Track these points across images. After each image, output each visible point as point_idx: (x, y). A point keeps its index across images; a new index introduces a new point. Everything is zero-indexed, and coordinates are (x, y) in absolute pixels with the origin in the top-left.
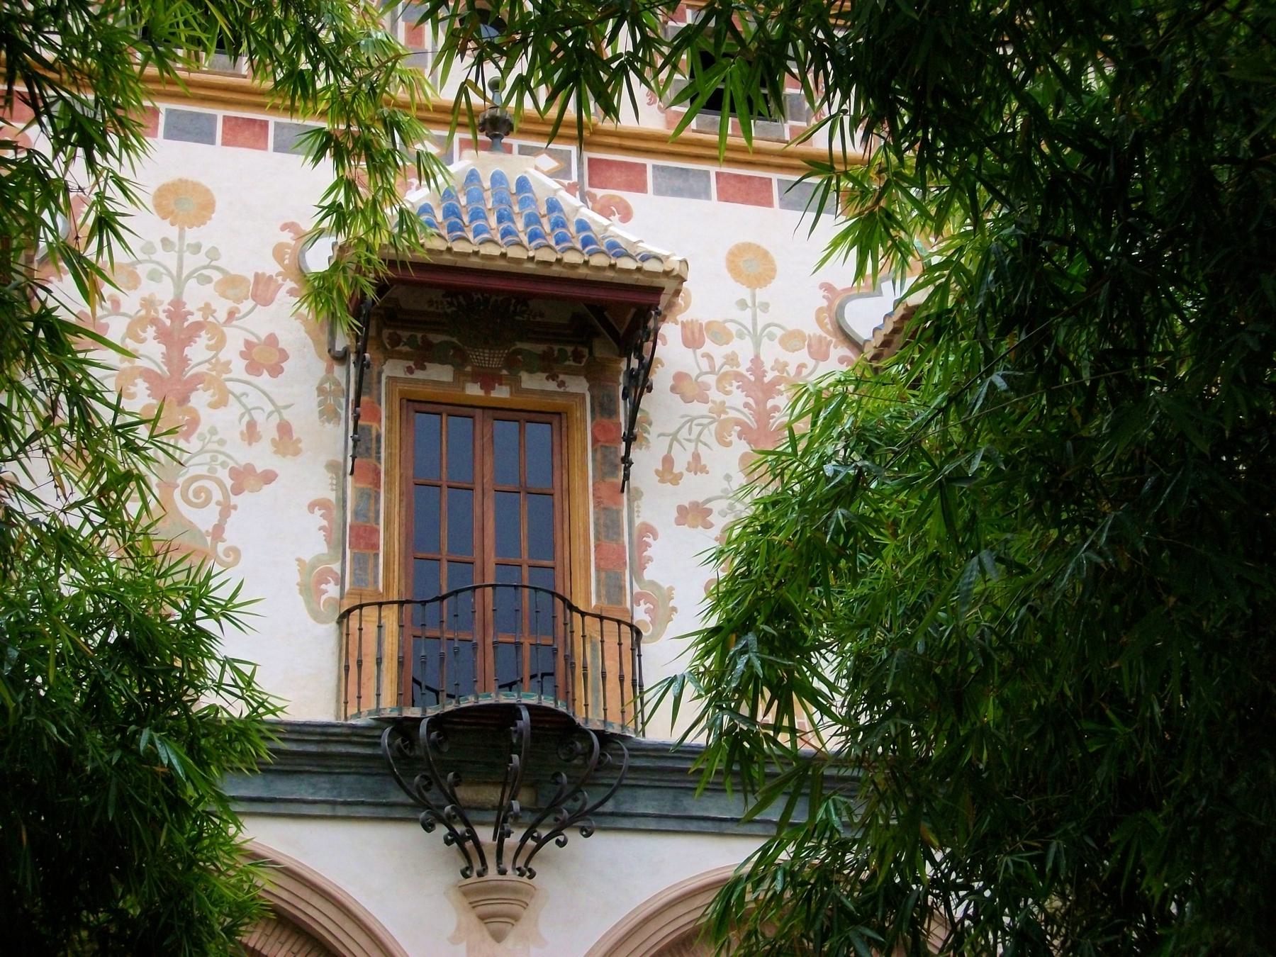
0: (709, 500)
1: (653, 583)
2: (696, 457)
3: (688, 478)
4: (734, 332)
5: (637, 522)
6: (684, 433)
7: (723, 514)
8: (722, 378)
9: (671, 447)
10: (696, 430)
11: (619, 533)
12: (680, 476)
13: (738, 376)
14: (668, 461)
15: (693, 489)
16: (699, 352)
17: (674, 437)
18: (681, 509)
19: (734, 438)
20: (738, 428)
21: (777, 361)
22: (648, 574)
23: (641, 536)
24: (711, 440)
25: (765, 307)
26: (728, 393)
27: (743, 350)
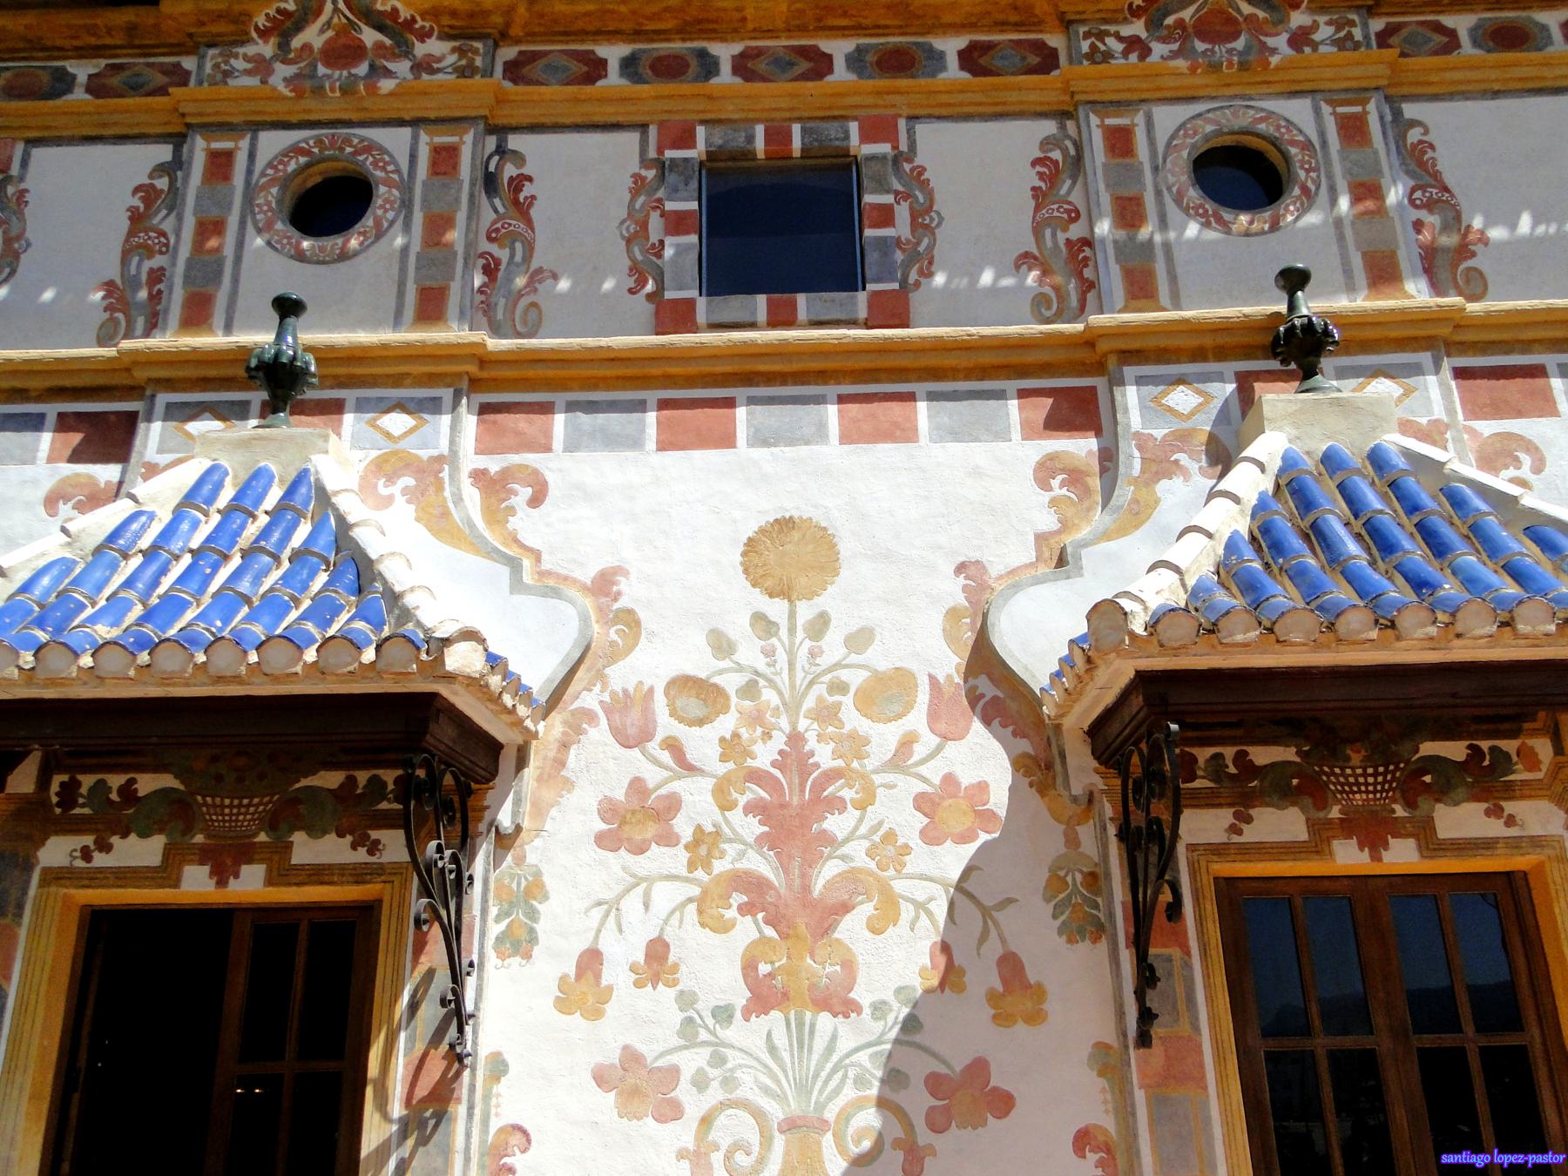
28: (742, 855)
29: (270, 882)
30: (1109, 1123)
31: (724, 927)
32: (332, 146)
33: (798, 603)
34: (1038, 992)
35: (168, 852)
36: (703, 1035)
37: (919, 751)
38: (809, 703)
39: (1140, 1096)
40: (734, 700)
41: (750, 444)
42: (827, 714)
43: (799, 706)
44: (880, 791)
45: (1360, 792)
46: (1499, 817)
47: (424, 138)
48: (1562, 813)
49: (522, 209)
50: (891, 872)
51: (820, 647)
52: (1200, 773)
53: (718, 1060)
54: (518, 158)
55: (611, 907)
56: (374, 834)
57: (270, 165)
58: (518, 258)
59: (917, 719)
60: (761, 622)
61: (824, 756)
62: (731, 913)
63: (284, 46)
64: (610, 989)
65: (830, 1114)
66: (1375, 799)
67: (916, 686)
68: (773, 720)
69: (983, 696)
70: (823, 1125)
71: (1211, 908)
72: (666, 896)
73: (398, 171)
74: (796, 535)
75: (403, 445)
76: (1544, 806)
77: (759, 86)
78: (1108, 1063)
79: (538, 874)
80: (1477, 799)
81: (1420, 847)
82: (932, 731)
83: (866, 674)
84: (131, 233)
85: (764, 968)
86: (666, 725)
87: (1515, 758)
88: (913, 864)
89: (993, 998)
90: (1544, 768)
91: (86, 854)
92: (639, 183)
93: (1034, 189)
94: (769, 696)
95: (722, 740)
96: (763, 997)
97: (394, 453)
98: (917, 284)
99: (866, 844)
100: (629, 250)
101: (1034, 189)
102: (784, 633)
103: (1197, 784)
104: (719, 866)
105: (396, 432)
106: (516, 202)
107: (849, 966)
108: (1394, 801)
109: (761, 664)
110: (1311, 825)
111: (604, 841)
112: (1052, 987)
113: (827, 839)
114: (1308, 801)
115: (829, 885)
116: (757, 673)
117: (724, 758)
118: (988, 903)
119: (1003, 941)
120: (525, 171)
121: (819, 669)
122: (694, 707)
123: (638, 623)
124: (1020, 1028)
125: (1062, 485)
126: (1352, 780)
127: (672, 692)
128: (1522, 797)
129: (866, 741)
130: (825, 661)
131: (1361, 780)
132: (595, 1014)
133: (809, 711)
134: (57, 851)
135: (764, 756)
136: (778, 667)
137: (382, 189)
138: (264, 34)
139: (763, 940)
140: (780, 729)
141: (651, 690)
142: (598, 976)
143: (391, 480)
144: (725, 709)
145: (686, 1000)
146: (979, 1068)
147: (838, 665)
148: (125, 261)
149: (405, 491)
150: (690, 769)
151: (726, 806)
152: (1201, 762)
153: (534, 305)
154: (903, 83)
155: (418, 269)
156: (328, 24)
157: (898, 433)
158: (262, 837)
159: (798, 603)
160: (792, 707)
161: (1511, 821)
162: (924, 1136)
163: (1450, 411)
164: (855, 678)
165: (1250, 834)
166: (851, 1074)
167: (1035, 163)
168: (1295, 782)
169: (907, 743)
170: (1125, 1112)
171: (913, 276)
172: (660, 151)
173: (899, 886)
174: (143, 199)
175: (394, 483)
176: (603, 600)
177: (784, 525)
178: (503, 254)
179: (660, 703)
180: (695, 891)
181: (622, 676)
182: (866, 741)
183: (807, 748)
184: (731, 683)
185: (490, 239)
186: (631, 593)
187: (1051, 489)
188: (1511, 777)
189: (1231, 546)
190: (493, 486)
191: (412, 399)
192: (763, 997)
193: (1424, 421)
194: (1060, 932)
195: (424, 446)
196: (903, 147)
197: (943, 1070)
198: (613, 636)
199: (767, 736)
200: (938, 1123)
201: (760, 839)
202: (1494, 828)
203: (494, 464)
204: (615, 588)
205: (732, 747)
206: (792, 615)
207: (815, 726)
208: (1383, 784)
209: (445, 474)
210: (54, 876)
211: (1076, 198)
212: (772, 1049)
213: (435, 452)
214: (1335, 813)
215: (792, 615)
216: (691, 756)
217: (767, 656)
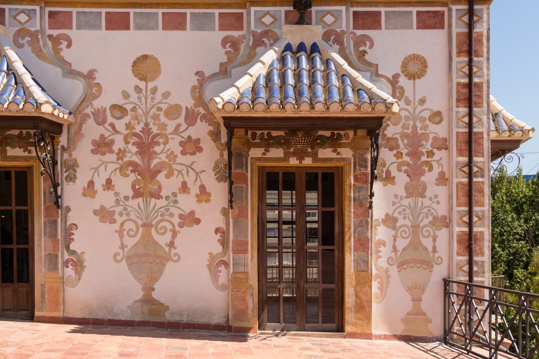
28: (131, 157)
30: (224, 227)
31: (127, 176)
33: (148, 83)
34: (209, 195)
36: (121, 203)
37: (182, 129)
38: (151, 114)
39: (231, 220)
40: (129, 112)
41: (135, 29)
42: (156, 117)
43: (148, 114)
44: (170, 140)
45: (300, 144)
46: (335, 152)
48: (352, 152)
50: (172, 162)
51: (155, 97)
52: (257, 138)
53: (125, 209)
55: (96, 169)
56: (29, 148)
59: (181, 120)
60: (138, 89)
61: (155, 130)
62: (129, 172)
64: (97, 191)
65: (154, 223)
66: (303, 146)
67: (182, 109)
68: (140, 119)
69: (201, 113)
70: (152, 226)
71: (256, 175)
72: (111, 167)
74: (148, 61)
75: (25, 26)
76: (348, 150)
78: (225, 212)
79: (76, 160)
80: (330, 147)
81: (313, 160)
82: (186, 123)
83: (167, 106)
85: (137, 187)
86: (110, 119)
87: (343, 136)
88: (178, 160)
89: (197, 196)
90: (350, 139)
94: (139, 111)
95: (126, 124)
96: (137, 194)
97: (23, 29)
99: (166, 154)
102: (144, 92)
103: (256, 141)
104: (125, 159)
105: (23, 21)
107: (160, 188)
108: (309, 147)
111: (93, 151)
112: (213, 194)
113: (155, 153)
114: (285, 146)
115: (155, 165)
116: (136, 104)
117: (127, 129)
118: (198, 171)
119: (201, 181)
121: (154, 104)
122: (118, 114)
123: (101, 87)
124: (204, 203)
125: (229, 47)
126: (298, 141)
127: (112, 109)
128: (342, 147)
129: (167, 125)
130: (156, 101)
131: (301, 141)
132: (93, 196)
133: (151, 116)
135: (138, 129)
136: (142, 102)
139: (137, 179)
140: (143, 121)
141: (105, 108)
142: (93, 188)
143: (23, 38)
144: (127, 114)
145: (117, 194)
146: (192, 213)
147: (159, 103)
150: (117, 132)
151: (127, 143)
152: (258, 135)
157: (180, 27)
159: (148, 83)
160: (146, 114)
161: (338, 153)
162: (177, 228)
164: (164, 107)
165: (268, 155)
166: (160, 213)
168: (282, 141)
169: (178, 126)
170: (228, 224)
173: (174, 166)
175: (24, 39)
176: (91, 80)
177: (145, 57)
179: (108, 112)
180: (119, 166)
181: (97, 104)
182: (167, 125)
183: (150, 127)
184: (129, 107)
187: (226, 48)
188: (341, 142)
191: (27, 10)
192: (137, 194)
193: (339, 30)
194: (216, 180)
195: (32, 26)
197: (183, 213)
198: (94, 91)
199: (139, 123)
200: (181, 225)
201: (137, 152)
202: (334, 155)
203: (55, 33)
204: (94, 76)
205: (128, 126)
206: (146, 87)
207: (152, 121)
208: (306, 142)
209: (40, 37)
212: (139, 207)
213: (36, 29)
214: (292, 150)
215: (146, 87)
216: (117, 129)
217: (139, 99)
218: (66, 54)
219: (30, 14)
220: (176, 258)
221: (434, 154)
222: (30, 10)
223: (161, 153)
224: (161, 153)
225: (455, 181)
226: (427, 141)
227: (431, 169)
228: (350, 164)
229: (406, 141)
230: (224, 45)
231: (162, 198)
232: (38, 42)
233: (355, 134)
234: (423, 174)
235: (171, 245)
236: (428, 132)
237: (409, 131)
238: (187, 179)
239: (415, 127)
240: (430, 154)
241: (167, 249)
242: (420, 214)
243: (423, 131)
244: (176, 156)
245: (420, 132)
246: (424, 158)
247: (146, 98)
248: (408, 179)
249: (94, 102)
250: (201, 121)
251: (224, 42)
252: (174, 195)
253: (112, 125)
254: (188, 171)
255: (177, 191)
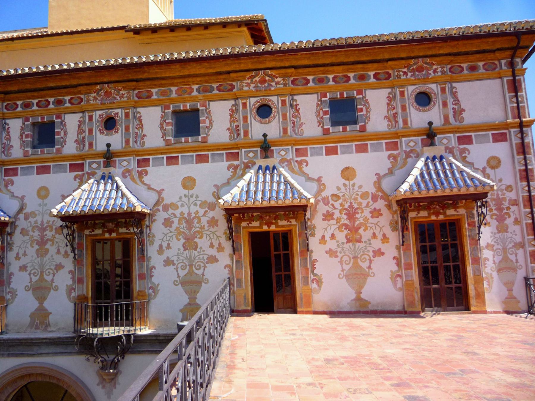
0: (27, 264)
1: (12, 288)
2: (25, 252)
3: (23, 258)
4: (37, 213)
5: (9, 272)
6: (22, 246)
7: (30, 267)
8: (33, 228)
9: (19, 250)
10: (25, 244)
11: (3, 277)
12: (20, 258)
13: (37, 227)
14: (18, 254)
15: (24, 261)
16: (28, 221)
17: (20, 247)
18: (20, 267)
19: (35, 245)
20: (36, 242)
21: (47, 221)
22: (11, 286)
23: (10, 275)
24: (29, 246)
25: (46, 205)
26: (34, 232)
27: (39, 218)
28: (344, 221)
29: (276, 227)
30: (398, 256)
31: (342, 231)
32: (264, 100)
34: (388, 239)
35: (260, 224)
36: (340, 246)
37: (370, 204)
38: (353, 197)
39: (402, 252)
40: (341, 197)
41: (341, 154)
42: (356, 199)
44: (364, 211)
47: (279, 98)
49: (298, 111)
53: (343, 249)
54: (296, 101)
55: (326, 229)
56: (290, 220)
57: (253, 105)
58: (298, 121)
59: (370, 199)
60: (345, 185)
61: (356, 206)
62: (343, 229)
63: (252, 80)
64: (327, 241)
65: (359, 256)
70: (358, 258)
71: (413, 226)
72: (333, 227)
73: (276, 105)
74: (349, 170)
75: (284, 157)
76: (463, 209)
77: (337, 85)
78: (398, 248)
79: (314, 225)
80: (453, 209)
83: (361, 193)
84: (231, 119)
85: (348, 237)
86: (331, 202)
88: (370, 221)
89: (382, 240)
91: (248, 224)
92: (318, 105)
93: (387, 103)
94: (347, 196)
96: (349, 241)
98: (367, 123)
99: (362, 219)
100: (317, 118)
101: (387, 103)
103: (412, 208)
104: (341, 223)
105: (283, 155)
106: (296, 110)
107: (361, 237)
109: (345, 191)
110: (429, 214)
111: (323, 220)
112: (390, 238)
113: (357, 218)
114: (428, 210)
115: (357, 225)
117: (340, 206)
118: (381, 226)
120: (297, 103)
122: (335, 199)
124: (386, 244)
129: (362, 203)
130: (355, 191)
132: (325, 244)
134: (244, 224)
135: (347, 206)
137: (274, 109)
138: (248, 79)
139: (348, 233)
142: (325, 239)
143: (283, 163)
145: (338, 242)
146: (380, 249)
147: (357, 191)
148: (231, 124)
149: (286, 165)
150: (335, 208)
151: (341, 213)
153: (302, 129)
154: (363, 82)
155: (282, 124)
156: (260, 77)
158: (274, 221)
160: (350, 198)
161: (458, 212)
162: (372, 258)
163: (455, 144)
164: (360, 193)
165: (419, 215)
167: (388, 97)
169: (368, 203)
170: (400, 254)
171: (367, 121)
172: (321, 98)
173: (368, 225)
174: (231, 112)
177: (347, 168)
178: (295, 120)
179: (330, 198)
180: (338, 226)
181: (324, 194)
184: (341, 195)
185: (293, 117)
186: (324, 181)
189: (417, 177)
190: (300, 163)
192: (349, 241)
193: (451, 147)
196: (364, 95)
198: (322, 188)
199: (347, 203)
200: (374, 257)
201: (347, 219)
202: (455, 213)
203: (299, 159)
205: (341, 205)
209: (292, 162)
210: (244, 228)
211: (394, 104)
212: (350, 248)
216: (335, 207)
218: (305, 169)
219: (286, 151)
220: (372, 275)
221: (510, 208)
222: (286, 149)
223: (360, 218)
224: (360, 218)
225: (524, 222)
226: (506, 201)
227: (509, 217)
228: (464, 217)
229: (494, 203)
230: (389, 159)
231: (362, 242)
232: (291, 164)
233: (466, 201)
234: (505, 219)
235: (370, 267)
236: (505, 196)
237: (495, 197)
238: (375, 231)
239: (498, 194)
240: (508, 208)
241: (367, 270)
242: (506, 241)
243: (503, 196)
244: (368, 219)
245: (501, 197)
246: (505, 211)
247: (350, 189)
248: (497, 223)
249: (322, 194)
250: (381, 199)
251: (389, 157)
252: (369, 240)
253: (332, 205)
254: (375, 227)
255: (370, 238)
